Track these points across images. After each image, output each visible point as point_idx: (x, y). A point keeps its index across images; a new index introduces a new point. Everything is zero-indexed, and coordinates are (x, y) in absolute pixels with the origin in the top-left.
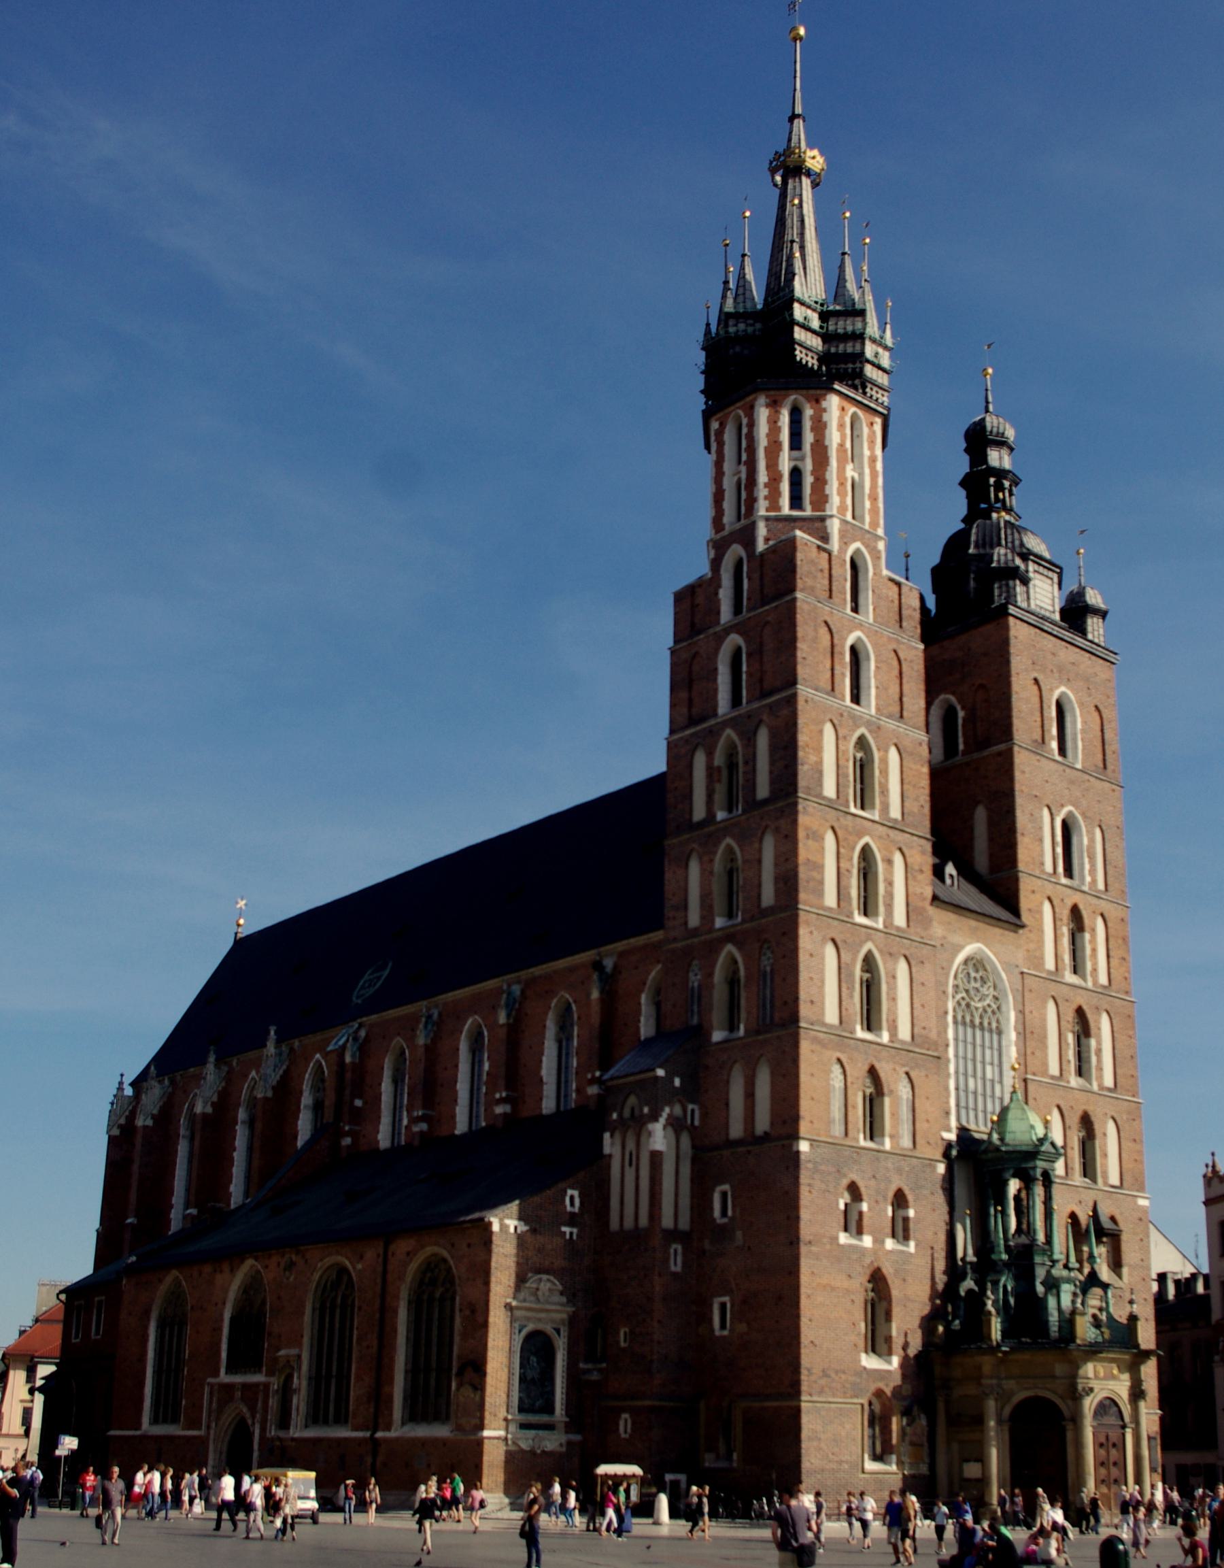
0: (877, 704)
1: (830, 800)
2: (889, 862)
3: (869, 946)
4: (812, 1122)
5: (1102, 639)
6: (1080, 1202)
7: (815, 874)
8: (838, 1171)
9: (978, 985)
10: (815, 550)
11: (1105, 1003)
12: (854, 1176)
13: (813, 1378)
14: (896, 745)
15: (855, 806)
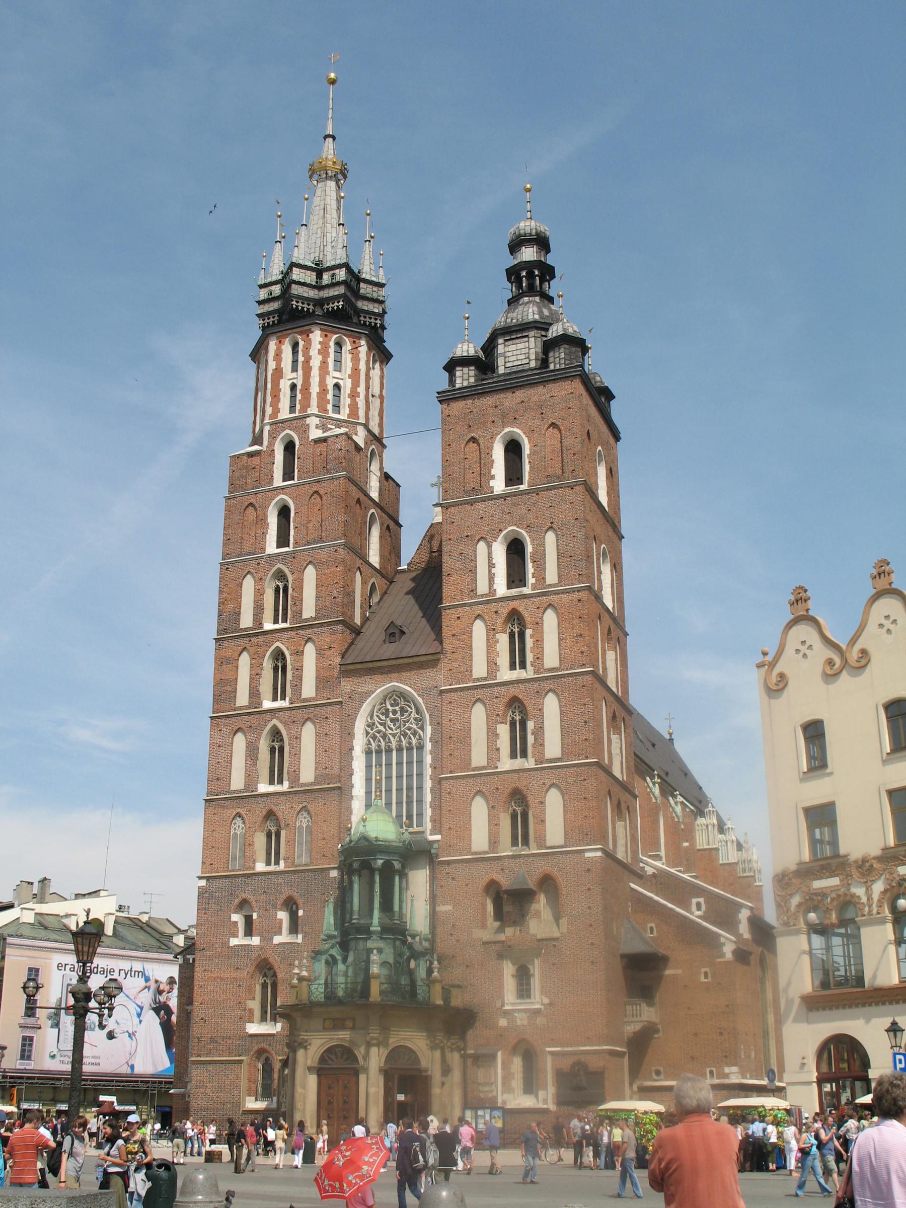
0: (295, 540)
1: (246, 629)
2: (299, 653)
3: (275, 722)
4: (211, 864)
5: (563, 361)
6: (502, 870)
7: (228, 688)
8: (231, 894)
9: (398, 715)
10: (245, 458)
11: (547, 685)
12: (244, 896)
13: (203, 1043)
14: (310, 562)
15: (276, 621)
